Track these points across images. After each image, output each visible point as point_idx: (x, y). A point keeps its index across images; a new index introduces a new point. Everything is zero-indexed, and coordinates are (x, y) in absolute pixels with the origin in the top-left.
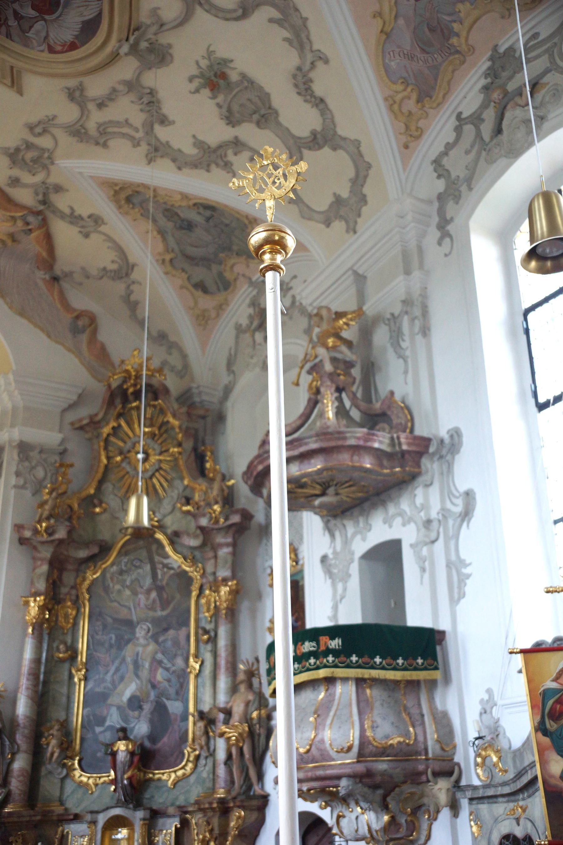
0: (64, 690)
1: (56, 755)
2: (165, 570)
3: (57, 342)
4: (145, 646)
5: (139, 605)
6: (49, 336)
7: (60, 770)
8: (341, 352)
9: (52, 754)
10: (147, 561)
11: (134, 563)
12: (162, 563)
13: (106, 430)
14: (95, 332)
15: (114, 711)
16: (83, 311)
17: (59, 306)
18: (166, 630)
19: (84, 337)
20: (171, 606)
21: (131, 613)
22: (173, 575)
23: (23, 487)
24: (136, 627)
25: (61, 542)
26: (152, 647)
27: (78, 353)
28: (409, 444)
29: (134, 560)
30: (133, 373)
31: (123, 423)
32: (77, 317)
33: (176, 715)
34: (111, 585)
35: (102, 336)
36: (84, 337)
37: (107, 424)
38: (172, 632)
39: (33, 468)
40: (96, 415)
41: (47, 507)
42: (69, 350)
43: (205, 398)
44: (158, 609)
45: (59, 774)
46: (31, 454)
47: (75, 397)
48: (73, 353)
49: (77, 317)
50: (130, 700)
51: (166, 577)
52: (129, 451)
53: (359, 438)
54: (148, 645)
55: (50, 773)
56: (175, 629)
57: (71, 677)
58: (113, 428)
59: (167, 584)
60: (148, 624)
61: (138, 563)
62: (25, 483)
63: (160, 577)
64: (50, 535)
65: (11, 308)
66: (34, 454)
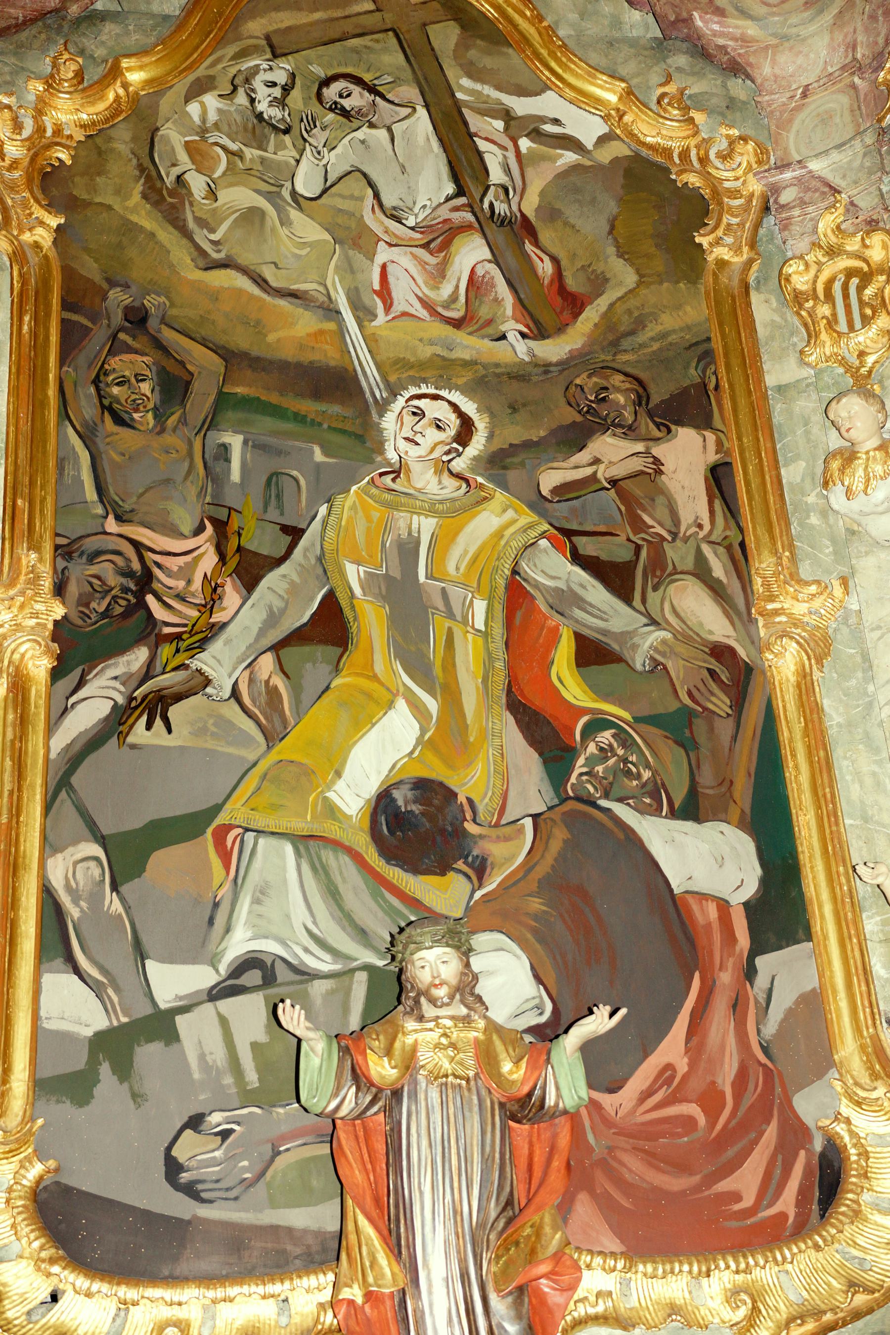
2: (525, 144)
5: (385, 293)
10: (410, 92)
11: (331, 92)
12: (507, 115)
20: (591, 316)
21: (342, 330)
22: (575, 168)
24: (383, 407)
29: (327, 82)
33: (723, 906)
34: (197, 183)
44: (512, 328)
51: (538, 181)
56: (630, 431)
59: (550, 212)
60: (455, 397)
61: (357, 99)
63: (496, 175)
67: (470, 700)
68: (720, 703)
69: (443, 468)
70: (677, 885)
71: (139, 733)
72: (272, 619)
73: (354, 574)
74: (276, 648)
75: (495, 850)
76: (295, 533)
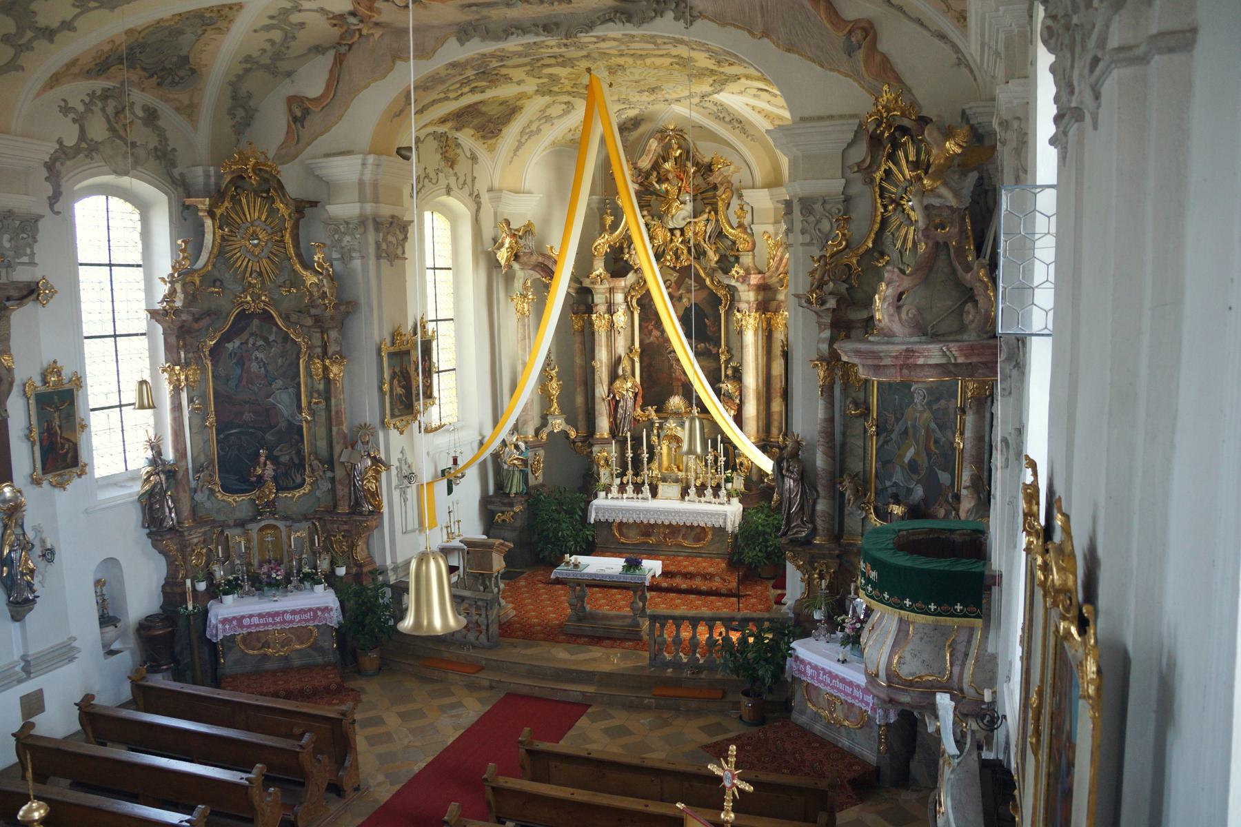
0: (860, 443)
1: (851, 502)
3: (831, 70)
4: (922, 412)
6: (822, 66)
7: (860, 512)
8: (940, 196)
9: (849, 500)
13: (879, 175)
14: (874, 41)
15: (898, 468)
16: (856, 21)
17: (828, 26)
18: (938, 399)
19: (860, 54)
23: (810, 244)
25: (834, 310)
26: (927, 415)
27: (857, 76)
28: (967, 356)
30: (885, 115)
31: (891, 165)
32: (850, 32)
35: (884, 46)
36: (860, 54)
37: (879, 168)
38: (943, 402)
39: (818, 222)
40: (864, 161)
41: (817, 276)
42: (846, 75)
43: (980, 119)
45: (859, 515)
46: (815, 206)
47: (851, 136)
48: (850, 77)
49: (850, 32)
50: (910, 461)
52: (902, 198)
53: (896, 357)
54: (925, 411)
55: (851, 513)
57: (865, 431)
58: (885, 170)
62: (812, 240)
64: (822, 305)
65: (778, 46)
66: (818, 207)
67: (921, 447)
68: (950, 453)
69: (921, 404)
70: (941, 481)
71: (885, 446)
72: (900, 430)
73: (909, 423)
74: (901, 434)
75: (921, 472)
76: (903, 414)
